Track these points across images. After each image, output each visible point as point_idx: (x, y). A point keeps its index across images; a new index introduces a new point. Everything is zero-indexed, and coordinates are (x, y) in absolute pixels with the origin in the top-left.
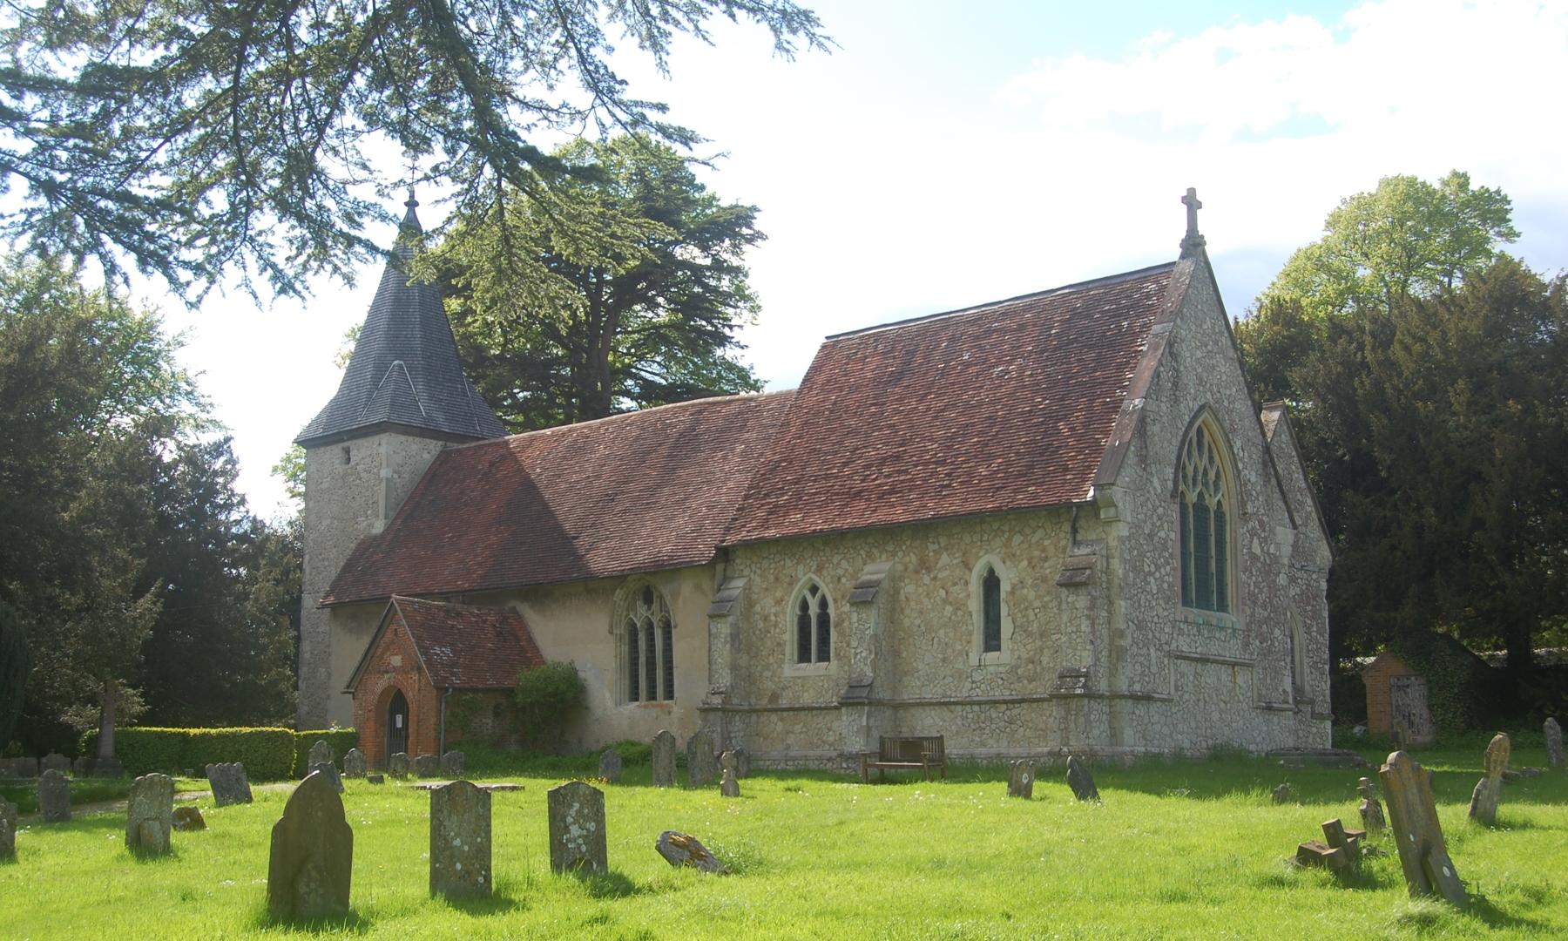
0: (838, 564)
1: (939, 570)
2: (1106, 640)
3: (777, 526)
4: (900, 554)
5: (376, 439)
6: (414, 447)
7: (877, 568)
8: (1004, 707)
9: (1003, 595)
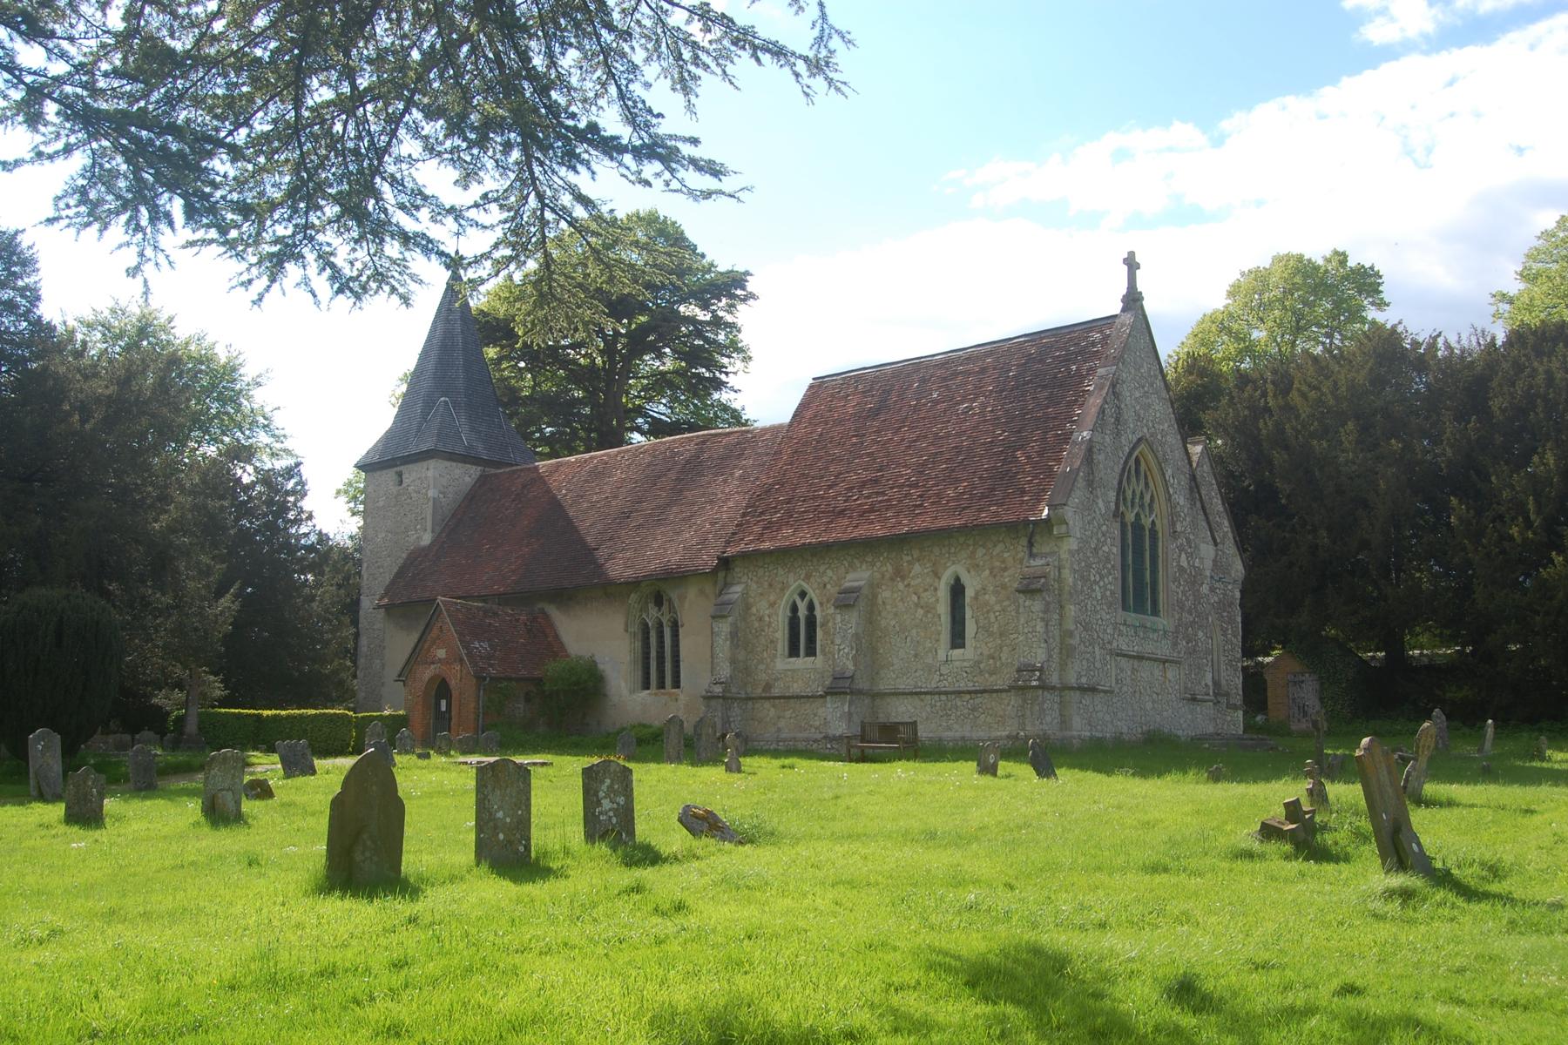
0: (824, 572)
1: (912, 578)
2: (1058, 639)
3: (771, 539)
4: (878, 564)
5: (425, 464)
6: (458, 471)
7: (859, 576)
8: (968, 696)
9: (967, 600)
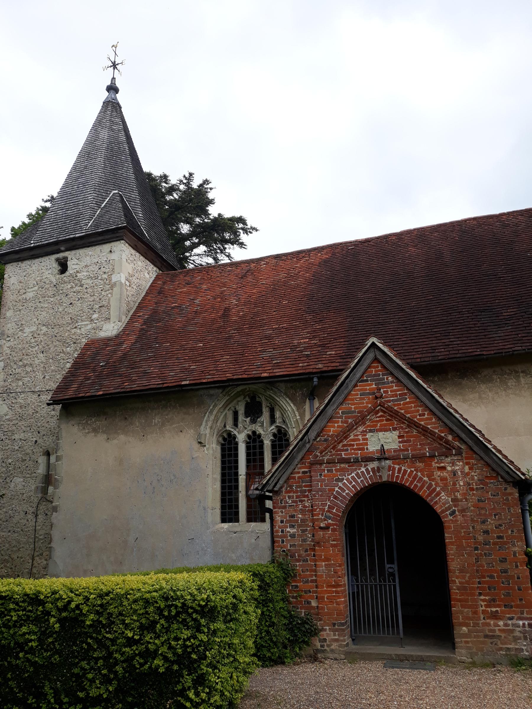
5: (106, 247)
6: (140, 263)
